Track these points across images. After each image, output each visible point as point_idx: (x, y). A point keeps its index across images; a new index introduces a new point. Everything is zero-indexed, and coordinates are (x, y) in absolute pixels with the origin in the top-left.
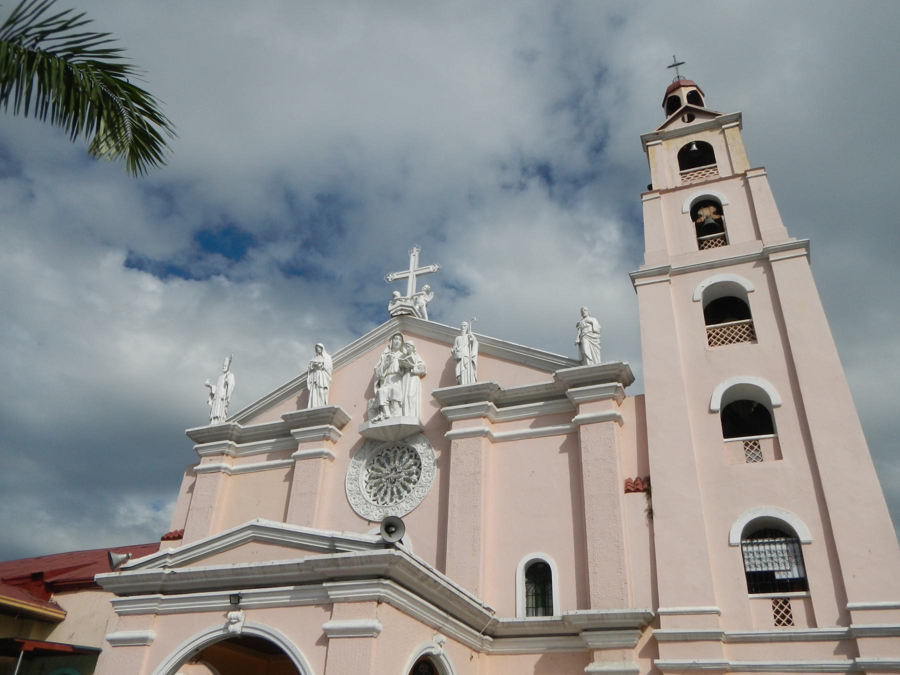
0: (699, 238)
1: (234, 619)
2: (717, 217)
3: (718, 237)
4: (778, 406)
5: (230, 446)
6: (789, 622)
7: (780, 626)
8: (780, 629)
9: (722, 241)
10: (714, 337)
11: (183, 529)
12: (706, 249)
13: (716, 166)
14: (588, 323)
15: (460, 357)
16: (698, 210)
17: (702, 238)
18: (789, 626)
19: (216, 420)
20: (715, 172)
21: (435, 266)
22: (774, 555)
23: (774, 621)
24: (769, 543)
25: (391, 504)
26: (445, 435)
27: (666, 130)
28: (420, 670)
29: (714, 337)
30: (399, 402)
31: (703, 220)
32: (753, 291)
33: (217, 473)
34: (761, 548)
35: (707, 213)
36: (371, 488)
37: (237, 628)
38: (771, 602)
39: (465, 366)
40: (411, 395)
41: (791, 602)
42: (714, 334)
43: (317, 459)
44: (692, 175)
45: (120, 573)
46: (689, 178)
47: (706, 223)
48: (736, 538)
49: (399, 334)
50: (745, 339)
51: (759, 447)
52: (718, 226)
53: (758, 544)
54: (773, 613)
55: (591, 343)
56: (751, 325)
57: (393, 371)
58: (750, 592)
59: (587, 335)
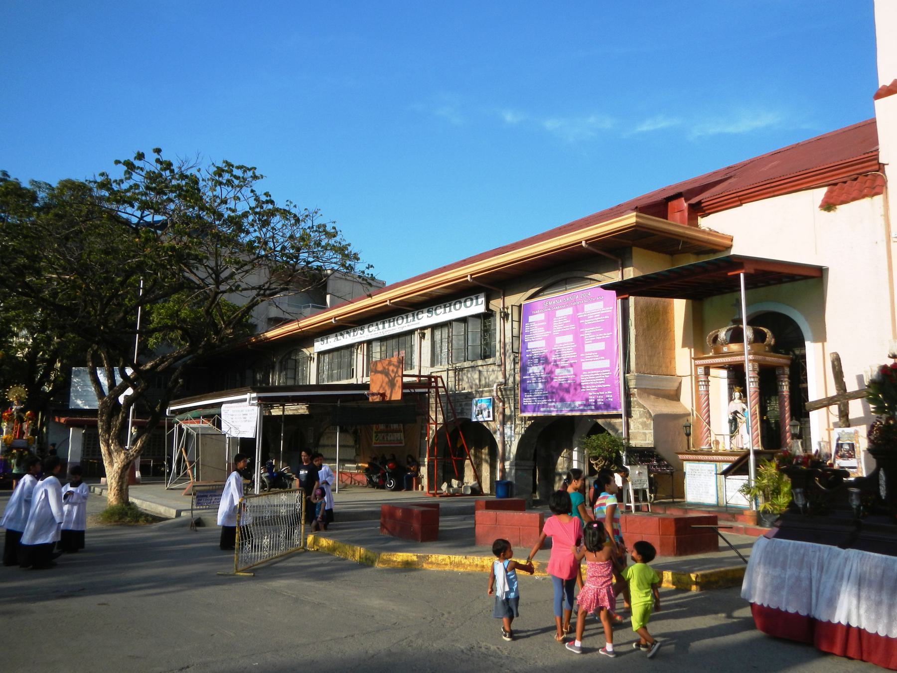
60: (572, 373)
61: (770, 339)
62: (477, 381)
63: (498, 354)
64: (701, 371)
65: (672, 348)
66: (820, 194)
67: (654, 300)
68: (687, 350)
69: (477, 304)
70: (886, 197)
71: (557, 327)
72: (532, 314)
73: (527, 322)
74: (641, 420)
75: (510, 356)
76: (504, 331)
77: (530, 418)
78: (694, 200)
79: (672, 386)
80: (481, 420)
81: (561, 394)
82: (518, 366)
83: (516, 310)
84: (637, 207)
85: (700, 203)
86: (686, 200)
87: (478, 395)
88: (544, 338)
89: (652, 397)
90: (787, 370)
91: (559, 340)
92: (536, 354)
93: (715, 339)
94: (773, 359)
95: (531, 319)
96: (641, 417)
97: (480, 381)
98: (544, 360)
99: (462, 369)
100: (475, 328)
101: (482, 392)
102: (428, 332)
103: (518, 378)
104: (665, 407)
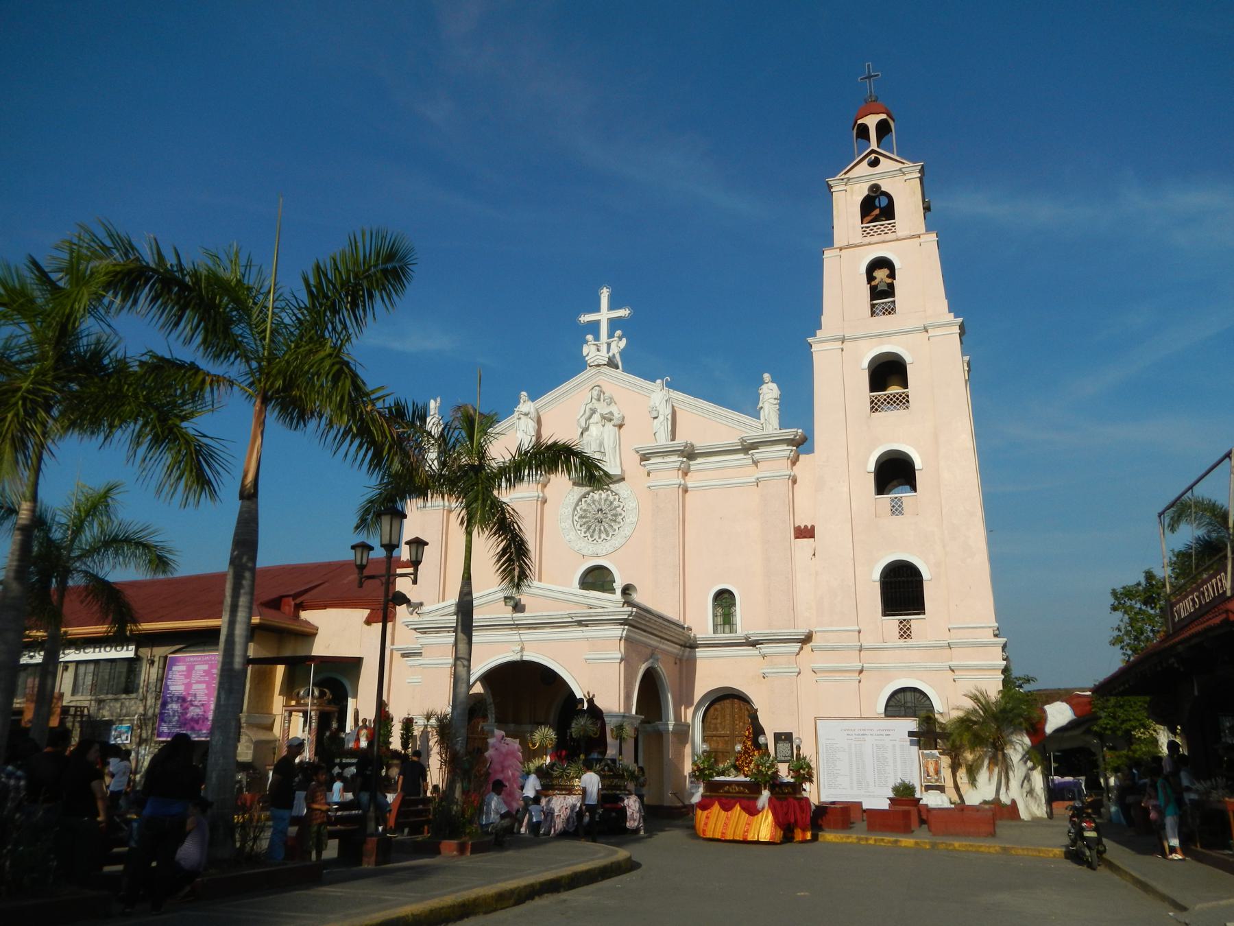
2: (889, 281)
3: (889, 302)
6: (909, 635)
7: (902, 640)
8: (902, 642)
10: (876, 404)
16: (874, 272)
17: (875, 302)
18: (908, 640)
20: (893, 228)
23: (898, 636)
25: (599, 541)
27: (850, 175)
29: (876, 404)
35: (881, 274)
36: (581, 526)
41: (912, 623)
42: (876, 401)
44: (872, 230)
46: (868, 233)
47: (879, 288)
52: (890, 291)
58: (885, 614)
60: (202, 710)
61: (329, 695)
62: (119, 710)
63: (141, 691)
64: (286, 714)
65: (272, 696)
66: (366, 612)
67: (264, 666)
68: (281, 697)
69: (127, 650)
70: (395, 623)
71: (195, 678)
72: (175, 665)
73: (171, 670)
74: (245, 744)
75: (151, 693)
76: (149, 674)
77: (163, 742)
78: (298, 601)
79: (268, 722)
80: (120, 742)
81: (192, 724)
82: (159, 702)
83: (162, 660)
84: (261, 603)
85: (302, 602)
86: (293, 600)
87: (118, 723)
88: (183, 684)
89: (255, 729)
90: (336, 715)
91: (195, 686)
92: (177, 694)
93: (298, 693)
94: (328, 708)
95: (175, 668)
96: (246, 742)
97: (121, 710)
98: (182, 699)
99: (104, 701)
100: (123, 668)
101: (122, 720)
102: (72, 668)
103: (157, 711)
104: (263, 736)
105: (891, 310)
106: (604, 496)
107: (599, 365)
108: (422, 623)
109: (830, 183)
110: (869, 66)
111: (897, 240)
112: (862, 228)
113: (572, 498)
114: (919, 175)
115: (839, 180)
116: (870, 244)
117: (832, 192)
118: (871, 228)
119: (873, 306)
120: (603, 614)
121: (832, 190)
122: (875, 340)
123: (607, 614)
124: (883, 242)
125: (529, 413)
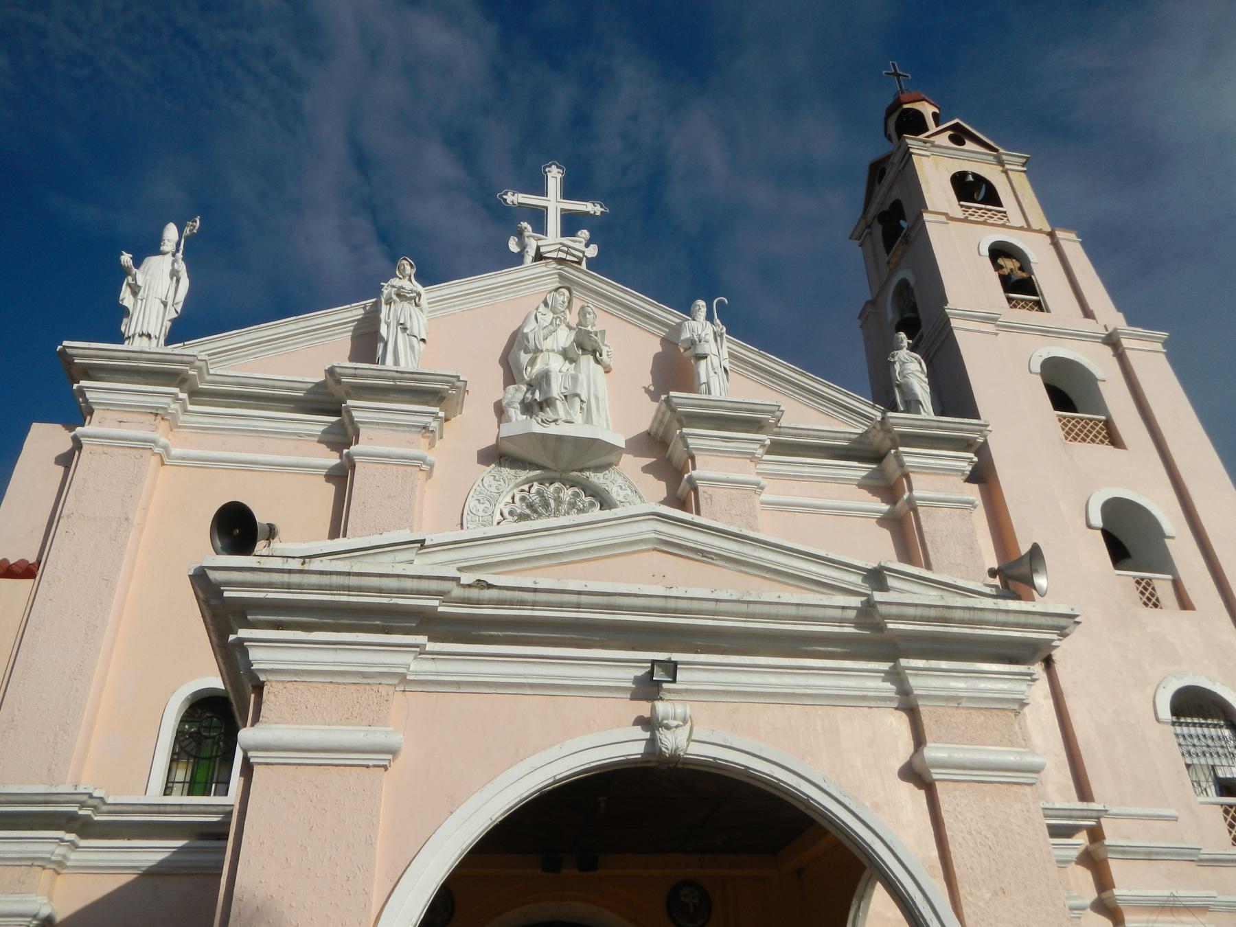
0: (1007, 294)
1: (675, 718)
2: (1025, 275)
3: (1030, 301)
4: (1172, 538)
5: (177, 399)
9: (1036, 308)
11: (32, 559)
12: (1019, 308)
13: (1005, 212)
14: (912, 357)
15: (707, 351)
19: (145, 339)
21: (595, 206)
22: (1210, 742)
24: (1201, 725)
26: (686, 476)
28: (683, 899)
30: (582, 401)
31: (1007, 273)
32: (1104, 381)
33: (141, 452)
34: (1192, 730)
35: (1009, 265)
37: (673, 741)
38: (1220, 810)
39: (713, 369)
40: (600, 396)
43: (408, 469)
45: (303, 563)
47: (1014, 278)
48: (1165, 713)
49: (569, 290)
50: (1102, 442)
51: (1153, 589)
53: (1187, 725)
54: (1225, 826)
55: (921, 386)
56: (1109, 425)
57: (555, 348)
59: (915, 375)
105: (1040, 306)
106: (567, 494)
107: (560, 261)
108: (295, 579)
109: (908, 141)
110: (893, 65)
111: (1021, 228)
112: (962, 206)
113: (495, 484)
114: (1025, 169)
115: (920, 140)
116: (984, 223)
117: (912, 153)
118: (974, 209)
119: (1010, 300)
120: (991, 617)
121: (911, 150)
122: (1037, 339)
123: (1002, 617)
124: (1003, 226)
125: (419, 295)
